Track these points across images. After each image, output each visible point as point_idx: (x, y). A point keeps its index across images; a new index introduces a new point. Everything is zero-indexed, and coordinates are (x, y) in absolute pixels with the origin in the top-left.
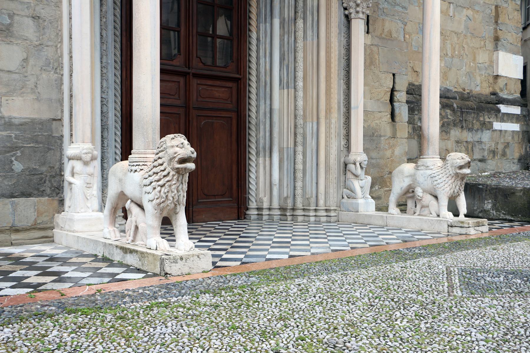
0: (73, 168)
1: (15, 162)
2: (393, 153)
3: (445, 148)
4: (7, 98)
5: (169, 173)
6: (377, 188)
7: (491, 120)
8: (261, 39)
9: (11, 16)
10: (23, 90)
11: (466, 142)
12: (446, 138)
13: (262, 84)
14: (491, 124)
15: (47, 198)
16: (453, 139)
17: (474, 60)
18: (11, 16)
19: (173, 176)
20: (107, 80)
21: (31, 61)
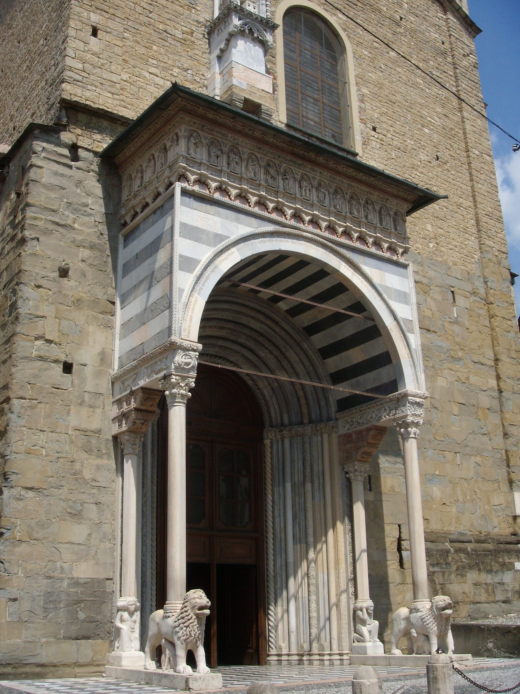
0: (122, 616)
1: (80, 612)
2: (404, 598)
3: (462, 591)
4: (76, 564)
5: (192, 617)
6: (389, 633)
7: (512, 560)
8: (276, 500)
9: (82, 504)
10: (87, 557)
11: (485, 584)
12: (462, 581)
13: (277, 540)
14: (512, 565)
15: (101, 640)
16: (470, 582)
17: (489, 503)
18: (82, 504)
19: (195, 619)
20: (146, 546)
21: (94, 536)
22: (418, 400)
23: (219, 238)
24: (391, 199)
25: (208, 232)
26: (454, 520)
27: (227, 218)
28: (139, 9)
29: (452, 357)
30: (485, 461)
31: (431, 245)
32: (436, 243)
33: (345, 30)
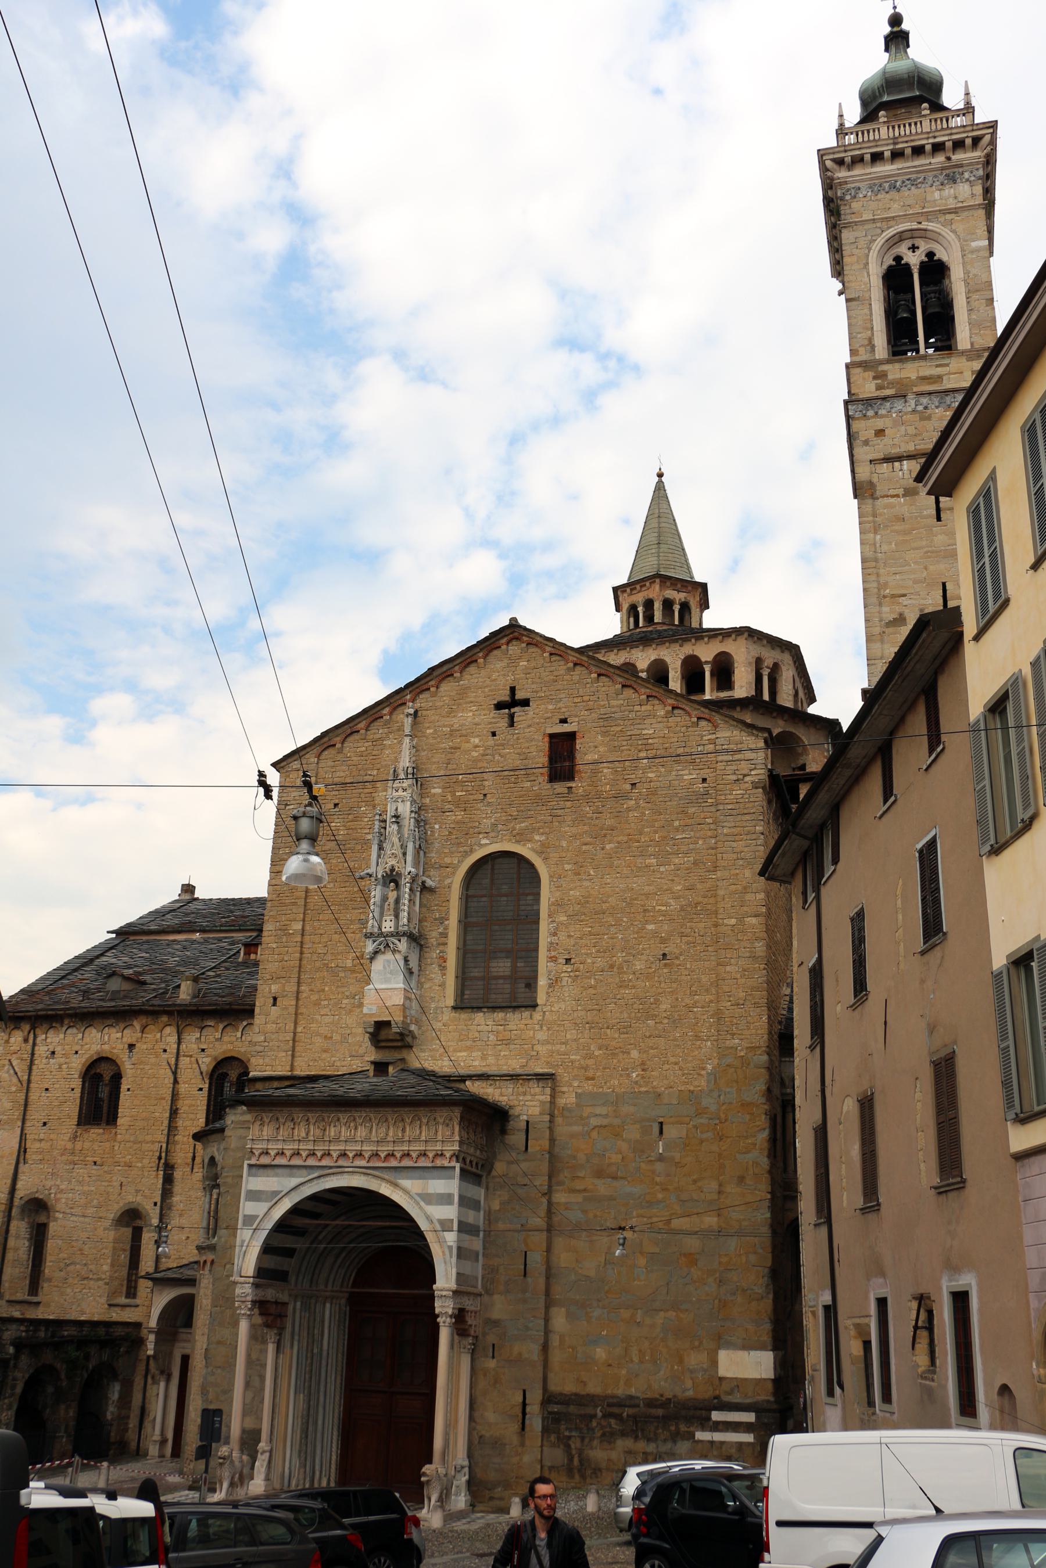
3: (606, 1458)
7: (692, 1429)
17: (681, 1361)
22: (444, 1293)
23: (275, 1193)
24: (439, 1109)
25: (267, 1191)
26: (622, 1383)
27: (283, 1176)
28: (315, 957)
29: (647, 1202)
30: (682, 1315)
31: (634, 1075)
32: (643, 1070)
33: (540, 853)
